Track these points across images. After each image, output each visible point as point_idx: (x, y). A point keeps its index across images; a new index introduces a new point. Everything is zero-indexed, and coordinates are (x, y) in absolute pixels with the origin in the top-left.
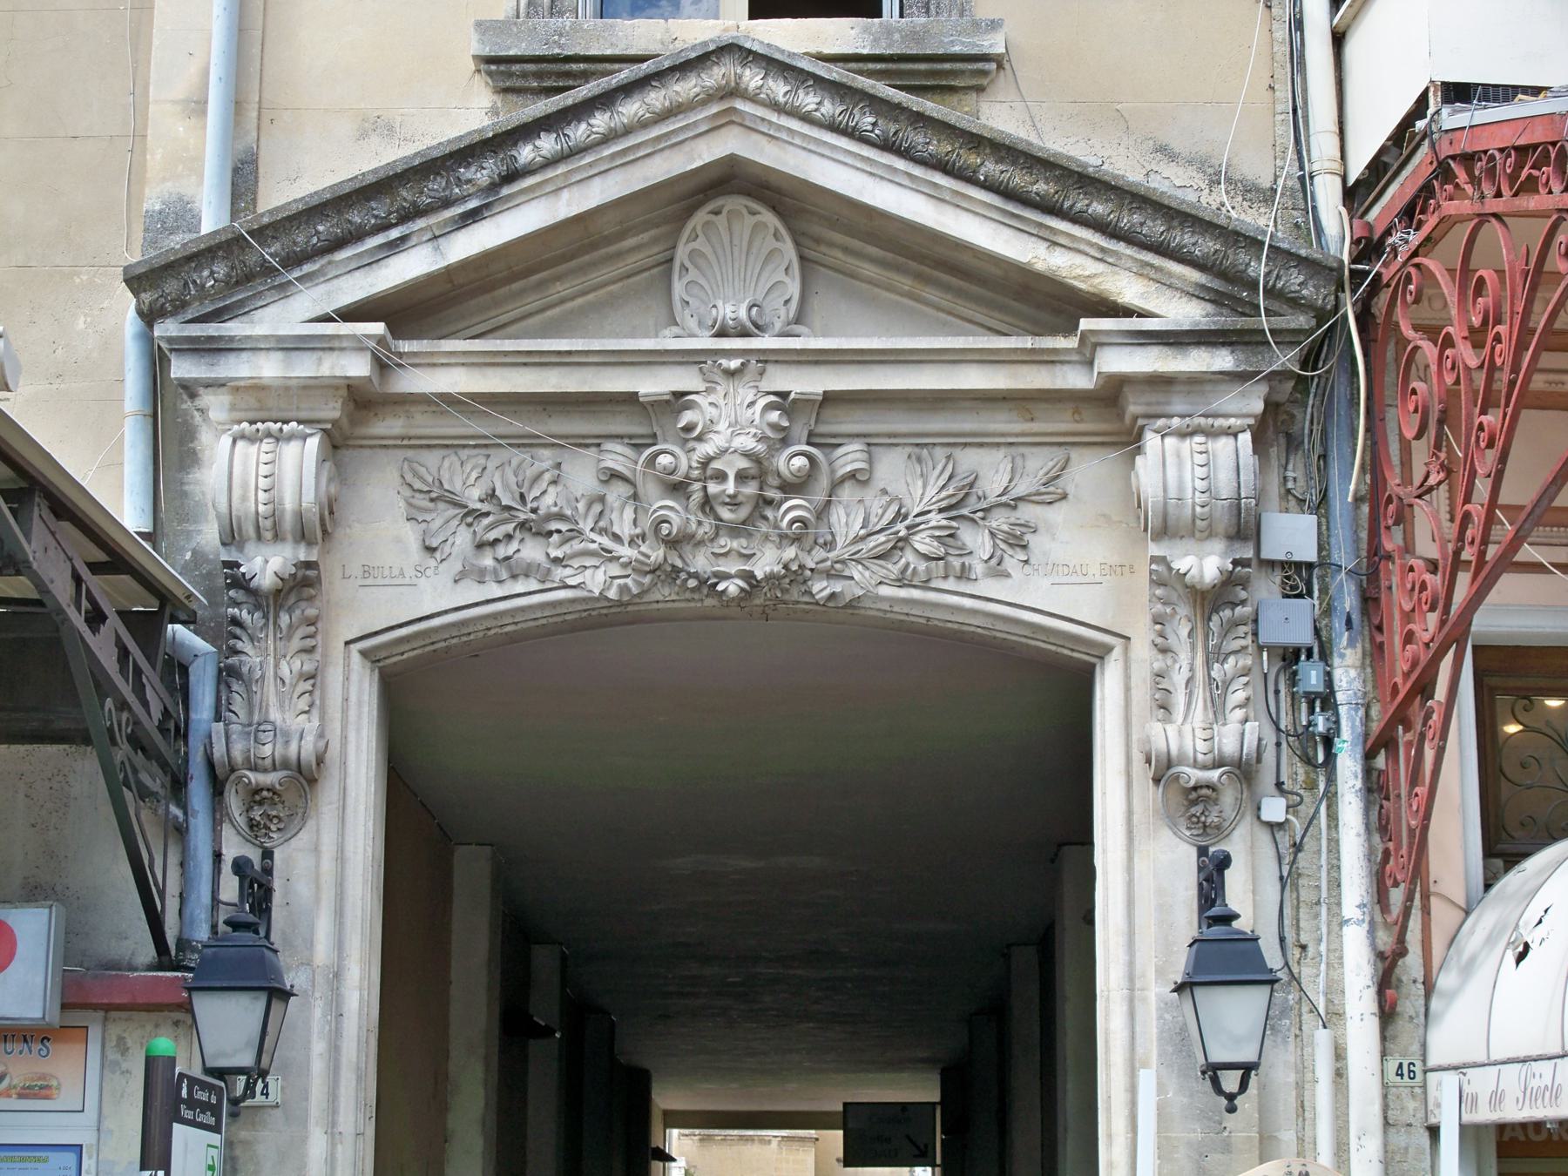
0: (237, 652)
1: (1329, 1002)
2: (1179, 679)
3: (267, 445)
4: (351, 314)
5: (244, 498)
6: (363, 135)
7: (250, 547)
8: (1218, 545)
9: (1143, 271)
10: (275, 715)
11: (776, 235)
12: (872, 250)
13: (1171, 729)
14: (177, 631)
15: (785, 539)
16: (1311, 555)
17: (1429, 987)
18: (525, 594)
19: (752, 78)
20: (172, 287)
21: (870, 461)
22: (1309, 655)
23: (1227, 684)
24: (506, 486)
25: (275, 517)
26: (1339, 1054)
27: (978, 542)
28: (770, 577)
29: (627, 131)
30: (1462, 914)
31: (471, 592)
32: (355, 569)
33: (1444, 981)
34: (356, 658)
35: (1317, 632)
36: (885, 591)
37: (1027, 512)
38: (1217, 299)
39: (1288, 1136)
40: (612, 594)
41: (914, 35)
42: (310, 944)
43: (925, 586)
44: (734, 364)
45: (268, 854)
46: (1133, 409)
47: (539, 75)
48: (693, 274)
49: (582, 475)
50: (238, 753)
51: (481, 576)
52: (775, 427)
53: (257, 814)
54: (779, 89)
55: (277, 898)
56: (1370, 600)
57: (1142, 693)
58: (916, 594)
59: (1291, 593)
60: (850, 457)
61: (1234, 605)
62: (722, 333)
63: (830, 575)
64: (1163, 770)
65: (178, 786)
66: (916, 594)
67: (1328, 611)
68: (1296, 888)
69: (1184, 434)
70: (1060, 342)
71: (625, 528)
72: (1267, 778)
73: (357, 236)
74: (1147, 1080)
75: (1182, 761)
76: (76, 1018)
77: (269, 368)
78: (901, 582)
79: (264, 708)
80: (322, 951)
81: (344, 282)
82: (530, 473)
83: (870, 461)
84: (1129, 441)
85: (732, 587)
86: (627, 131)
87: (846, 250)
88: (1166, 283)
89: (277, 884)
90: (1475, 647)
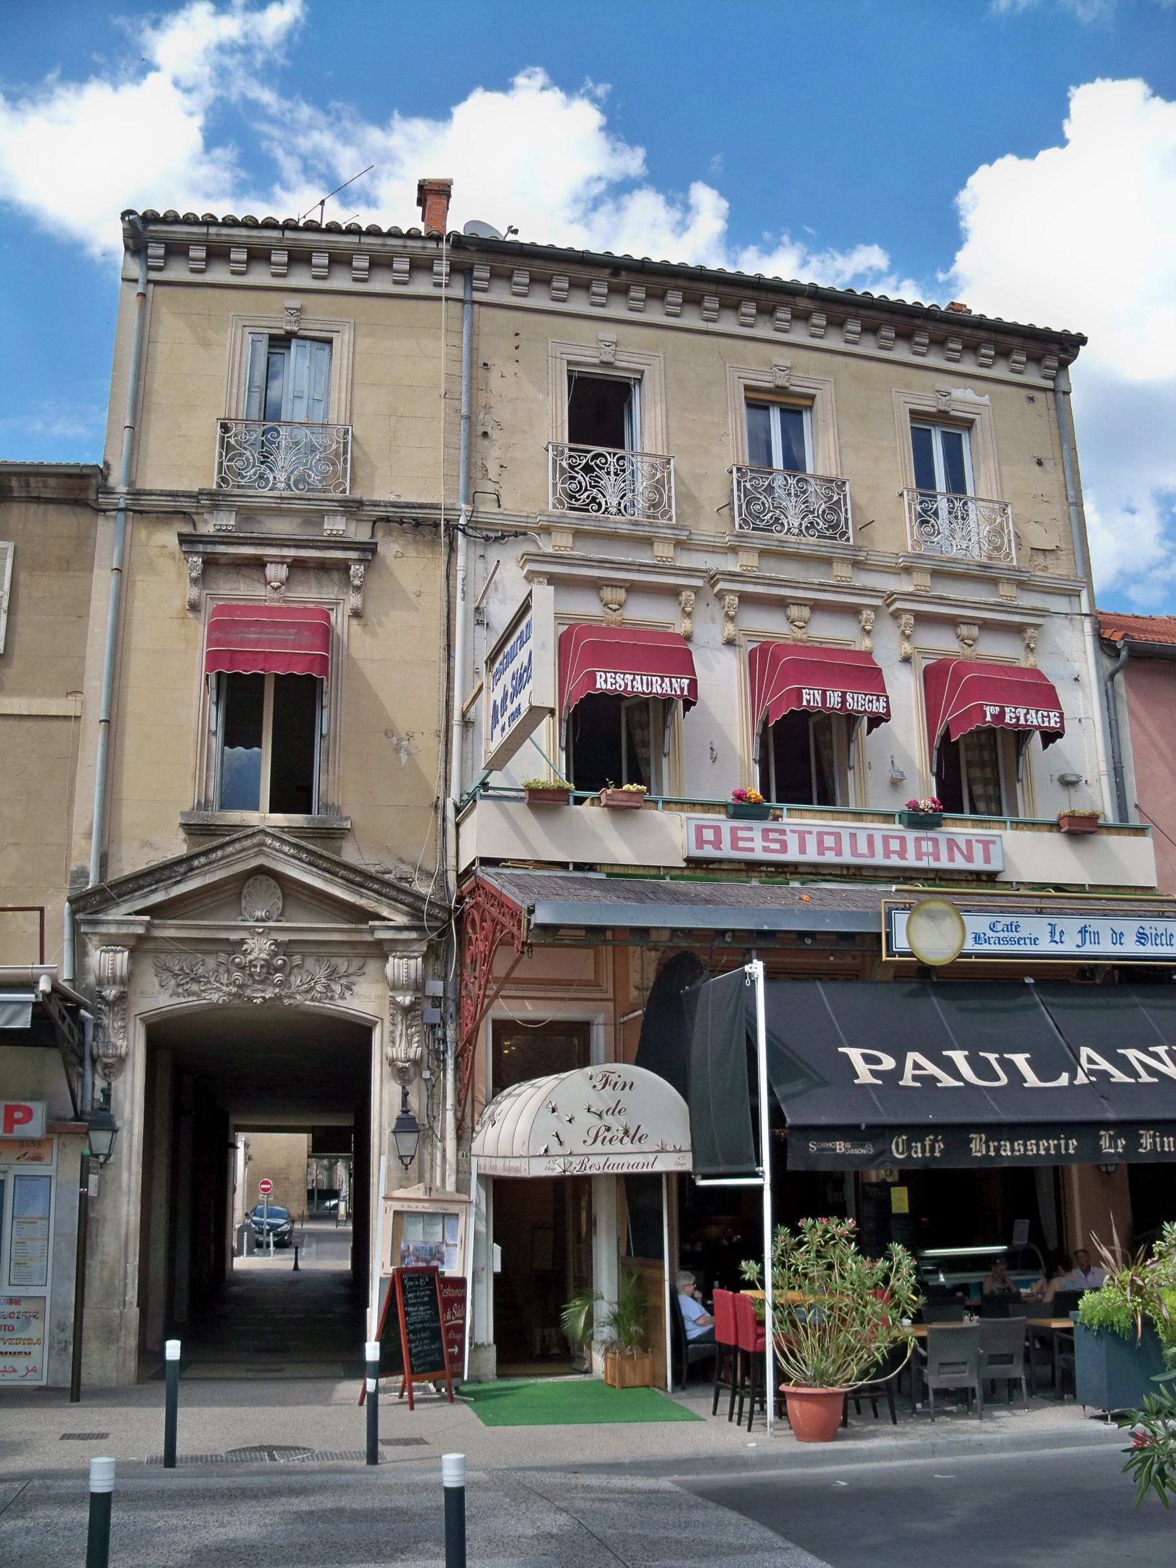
0: (100, 1019)
1: (441, 1134)
2: (398, 1033)
3: (111, 954)
4: (138, 913)
5: (104, 971)
6: (142, 847)
7: (105, 987)
8: (411, 993)
9: (389, 906)
10: (112, 1039)
11: (275, 887)
12: (306, 892)
13: (394, 1050)
14: (83, 1012)
15: (275, 986)
16: (441, 995)
17: (473, 1129)
18: (192, 1001)
19: (269, 841)
20: (82, 903)
21: (303, 961)
22: (439, 1026)
23: (412, 1036)
24: (187, 967)
25: (114, 976)
26: (444, 1150)
27: (337, 988)
28: (270, 998)
29: (228, 856)
30: (483, 1107)
31: (175, 1000)
32: (138, 992)
33: (478, 1128)
34: (138, 1021)
35: (442, 1018)
36: (307, 1003)
37: (353, 979)
38: (412, 916)
39: (427, 1175)
40: (220, 1002)
41: (322, 821)
42: (123, 1112)
43: (319, 1001)
44: (260, 930)
45: (110, 1084)
46: (385, 949)
47: (200, 830)
48: (248, 899)
49: (211, 963)
50: (101, 1052)
51: (178, 995)
52: (273, 951)
53: (107, 1071)
54: (277, 845)
55: (112, 1098)
56: (458, 1008)
57: (387, 1037)
58: (317, 1004)
59: (434, 1006)
60: (297, 960)
61: (415, 1011)
62: (257, 920)
63: (290, 997)
64: (392, 1062)
65: (81, 1062)
66: (317, 1004)
67: (446, 1011)
68: (432, 1098)
69: (401, 958)
70: (363, 926)
71: (225, 981)
72: (425, 1065)
73: (141, 888)
74: (384, 1159)
75: (397, 1059)
76: (51, 1136)
77: (113, 930)
78: (312, 1000)
79: (109, 1037)
80: (127, 1115)
81: (137, 902)
82: (194, 962)
83: (303, 961)
84: (385, 958)
85: (258, 1001)
86: (228, 856)
87: (298, 892)
88: (397, 910)
89: (113, 1093)
90: (494, 1022)
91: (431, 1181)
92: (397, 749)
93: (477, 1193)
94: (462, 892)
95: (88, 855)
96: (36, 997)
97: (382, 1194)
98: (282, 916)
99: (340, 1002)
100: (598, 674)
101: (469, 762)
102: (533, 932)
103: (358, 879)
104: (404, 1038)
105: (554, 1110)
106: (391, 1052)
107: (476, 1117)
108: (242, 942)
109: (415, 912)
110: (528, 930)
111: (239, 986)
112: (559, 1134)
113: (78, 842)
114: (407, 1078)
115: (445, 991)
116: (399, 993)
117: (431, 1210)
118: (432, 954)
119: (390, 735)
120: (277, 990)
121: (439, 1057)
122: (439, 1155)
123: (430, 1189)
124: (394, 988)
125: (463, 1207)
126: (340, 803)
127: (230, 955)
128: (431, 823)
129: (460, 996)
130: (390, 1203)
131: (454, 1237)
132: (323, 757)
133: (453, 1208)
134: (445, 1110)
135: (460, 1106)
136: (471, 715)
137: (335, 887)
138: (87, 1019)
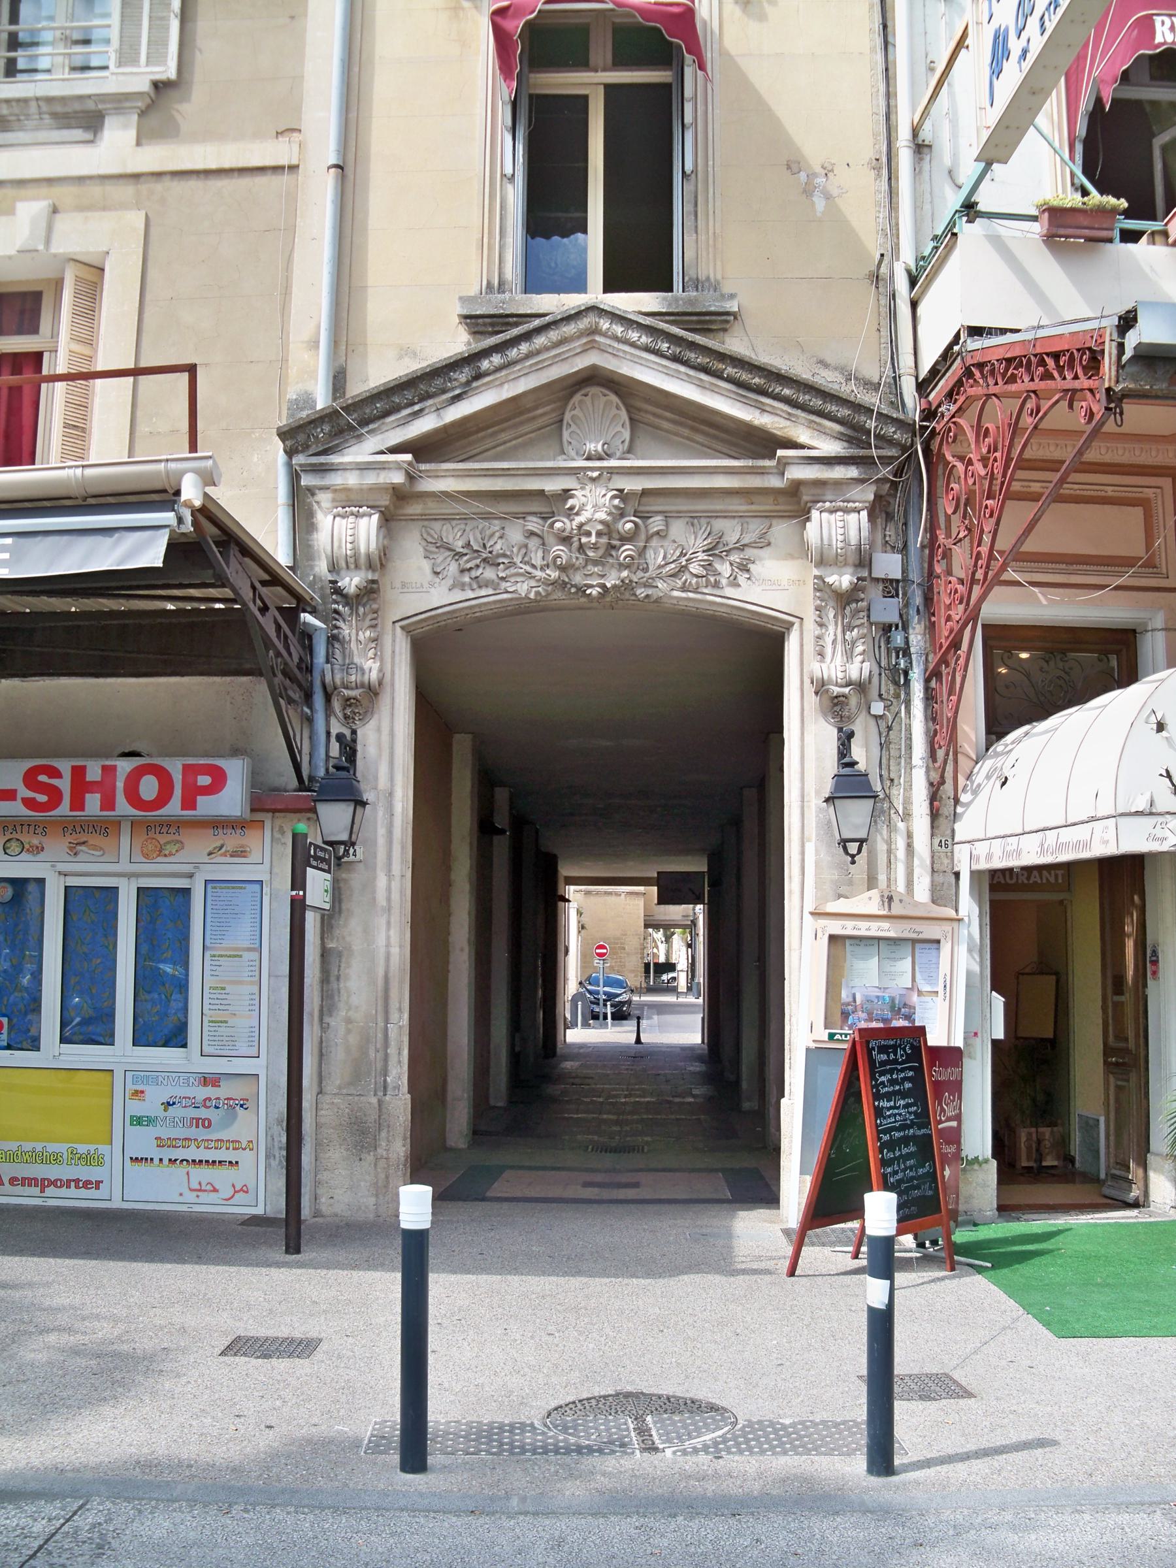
0: (337, 627)
1: (905, 808)
2: (829, 640)
3: (351, 519)
4: (394, 450)
5: (340, 547)
6: (401, 357)
7: (343, 573)
8: (850, 570)
9: (810, 425)
10: (356, 660)
11: (618, 408)
12: (668, 414)
13: (824, 666)
14: (306, 617)
15: (622, 566)
16: (899, 576)
17: (957, 801)
18: (486, 596)
19: (605, 324)
20: (301, 437)
21: (667, 525)
22: (897, 628)
23: (854, 643)
24: (476, 539)
25: (356, 556)
26: (909, 835)
27: (724, 569)
28: (614, 586)
29: (538, 352)
30: (973, 763)
31: (458, 595)
32: (398, 584)
33: (964, 798)
34: (398, 630)
35: (901, 616)
36: (676, 593)
37: (750, 553)
38: (850, 440)
39: (882, 878)
40: (532, 596)
41: (690, 302)
42: (376, 778)
43: (695, 591)
44: (595, 474)
45: (354, 732)
46: (805, 498)
47: (492, 325)
48: (573, 428)
49: (515, 535)
50: (338, 681)
51: (463, 586)
52: (616, 507)
53: (348, 711)
54: (618, 329)
55: (359, 755)
56: (928, 600)
57: (810, 647)
58: (691, 595)
59: (888, 595)
60: (656, 524)
61: (857, 601)
62: (589, 459)
63: (646, 585)
64: (821, 687)
65: (308, 697)
66: (691, 595)
67: (907, 605)
68: (888, 749)
69: (832, 511)
70: (767, 463)
71: (538, 562)
72: (874, 693)
73: (396, 409)
74: (810, 848)
75: (830, 682)
76: (259, 816)
77: (352, 479)
78: (684, 589)
79: (351, 654)
80: (383, 782)
81: (391, 434)
82: (488, 533)
83: (667, 525)
84: (803, 515)
85: (594, 592)
86: (538, 352)
87: (654, 415)
88: (823, 432)
89: (359, 748)
90: (983, 625)
91: (889, 886)
92: (808, 191)
93: (969, 907)
94: (930, 403)
95: (313, 375)
96: (180, 520)
97: (809, 906)
98: (630, 451)
99: (729, 592)
100: (1158, 20)
101: (927, 207)
102: (1127, 369)
103: (757, 380)
104: (839, 647)
105: (1161, 727)
106: (817, 668)
107: (961, 781)
108: (566, 494)
109: (855, 434)
110: (1120, 366)
111: (563, 569)
112: (1172, 773)
113: (299, 355)
114: (846, 713)
115: (904, 571)
116: (829, 570)
117: (892, 934)
118: (879, 510)
119: (795, 169)
120: (625, 574)
121: (899, 678)
122: (900, 843)
123: (890, 899)
124: (821, 562)
125: (947, 927)
126: (719, 277)
127: (545, 519)
128: (869, 301)
129: (931, 574)
130: (823, 922)
131: (931, 978)
132: (689, 207)
133: (931, 931)
134: (910, 767)
135: (934, 760)
136: (926, 134)
137: (717, 397)
138: (316, 629)
